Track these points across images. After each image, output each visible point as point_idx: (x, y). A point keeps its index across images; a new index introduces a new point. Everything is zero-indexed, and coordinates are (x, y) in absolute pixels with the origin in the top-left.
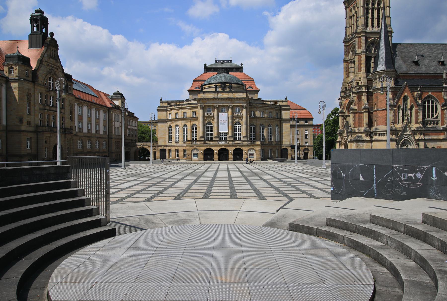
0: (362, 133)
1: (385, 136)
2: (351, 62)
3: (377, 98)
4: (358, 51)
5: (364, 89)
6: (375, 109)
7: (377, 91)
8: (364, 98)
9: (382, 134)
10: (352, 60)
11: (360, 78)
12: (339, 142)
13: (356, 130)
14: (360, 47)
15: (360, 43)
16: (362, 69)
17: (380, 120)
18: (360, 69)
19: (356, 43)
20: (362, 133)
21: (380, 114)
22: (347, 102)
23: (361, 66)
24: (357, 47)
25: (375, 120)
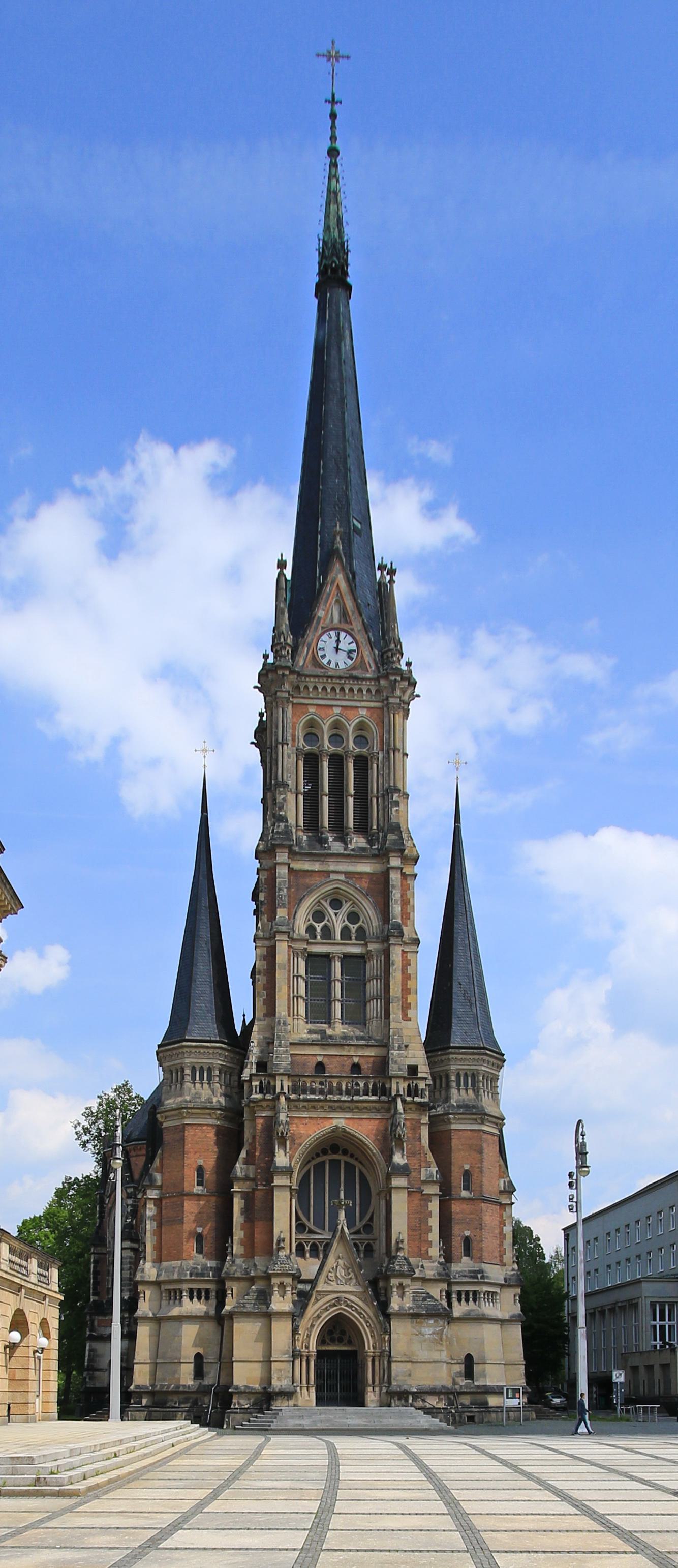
6: (464, 1194)
25: (467, 1241)
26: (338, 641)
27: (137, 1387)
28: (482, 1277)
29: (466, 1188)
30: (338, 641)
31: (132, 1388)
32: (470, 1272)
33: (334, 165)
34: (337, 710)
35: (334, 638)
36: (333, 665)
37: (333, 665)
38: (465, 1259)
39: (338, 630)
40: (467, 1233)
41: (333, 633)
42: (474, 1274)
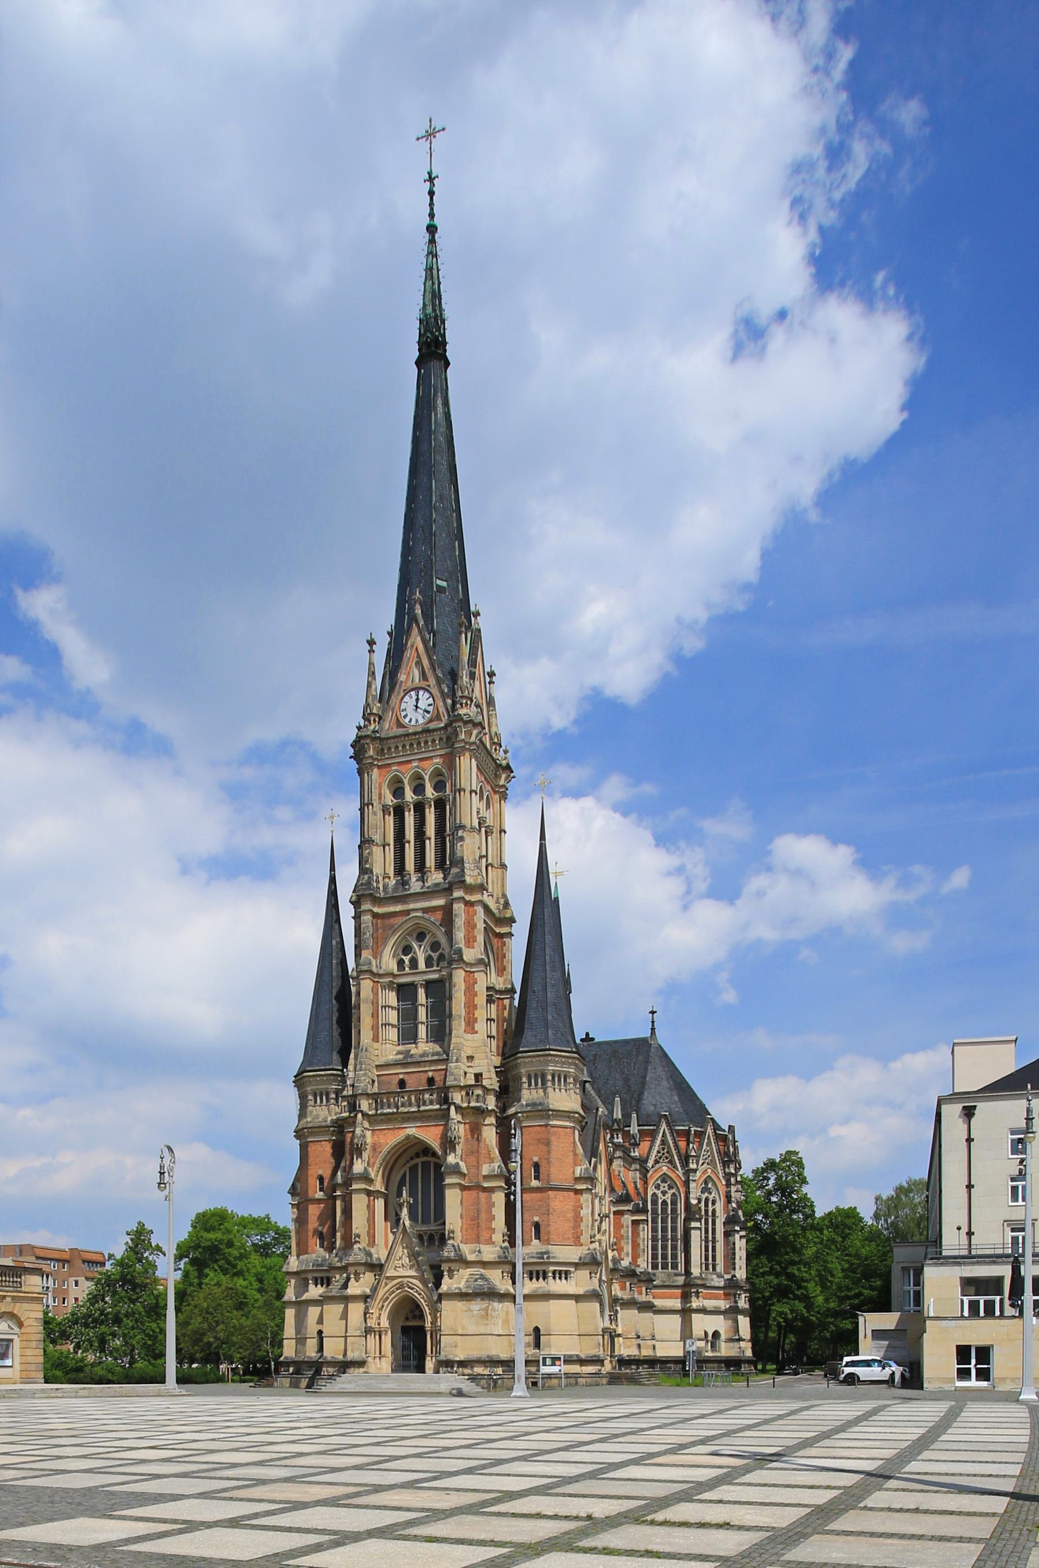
0: (485, 1264)
1: (572, 1281)
2: (390, 986)
3: (548, 1143)
4: (469, 955)
5: (491, 1103)
7: (548, 1117)
8: (490, 1134)
9: (560, 1272)
10: (394, 976)
11: (470, 1058)
12: (365, 1298)
13: (468, 1251)
14: (470, 941)
15: (470, 926)
16: (477, 1027)
17: (558, 1225)
18: (470, 1024)
19: (460, 922)
20: (485, 1264)
21: (560, 1202)
22: (391, 1138)
23: (468, 1013)
24: (460, 935)
26: (417, 700)
27: (286, 1358)
28: (548, 1258)
29: (537, 1178)
30: (417, 700)
31: (282, 1359)
32: (538, 1253)
33: (432, 241)
34: (415, 764)
35: (414, 697)
36: (413, 723)
37: (413, 723)
38: (535, 1242)
39: (417, 689)
40: (536, 1219)
41: (413, 693)
42: (541, 1255)
